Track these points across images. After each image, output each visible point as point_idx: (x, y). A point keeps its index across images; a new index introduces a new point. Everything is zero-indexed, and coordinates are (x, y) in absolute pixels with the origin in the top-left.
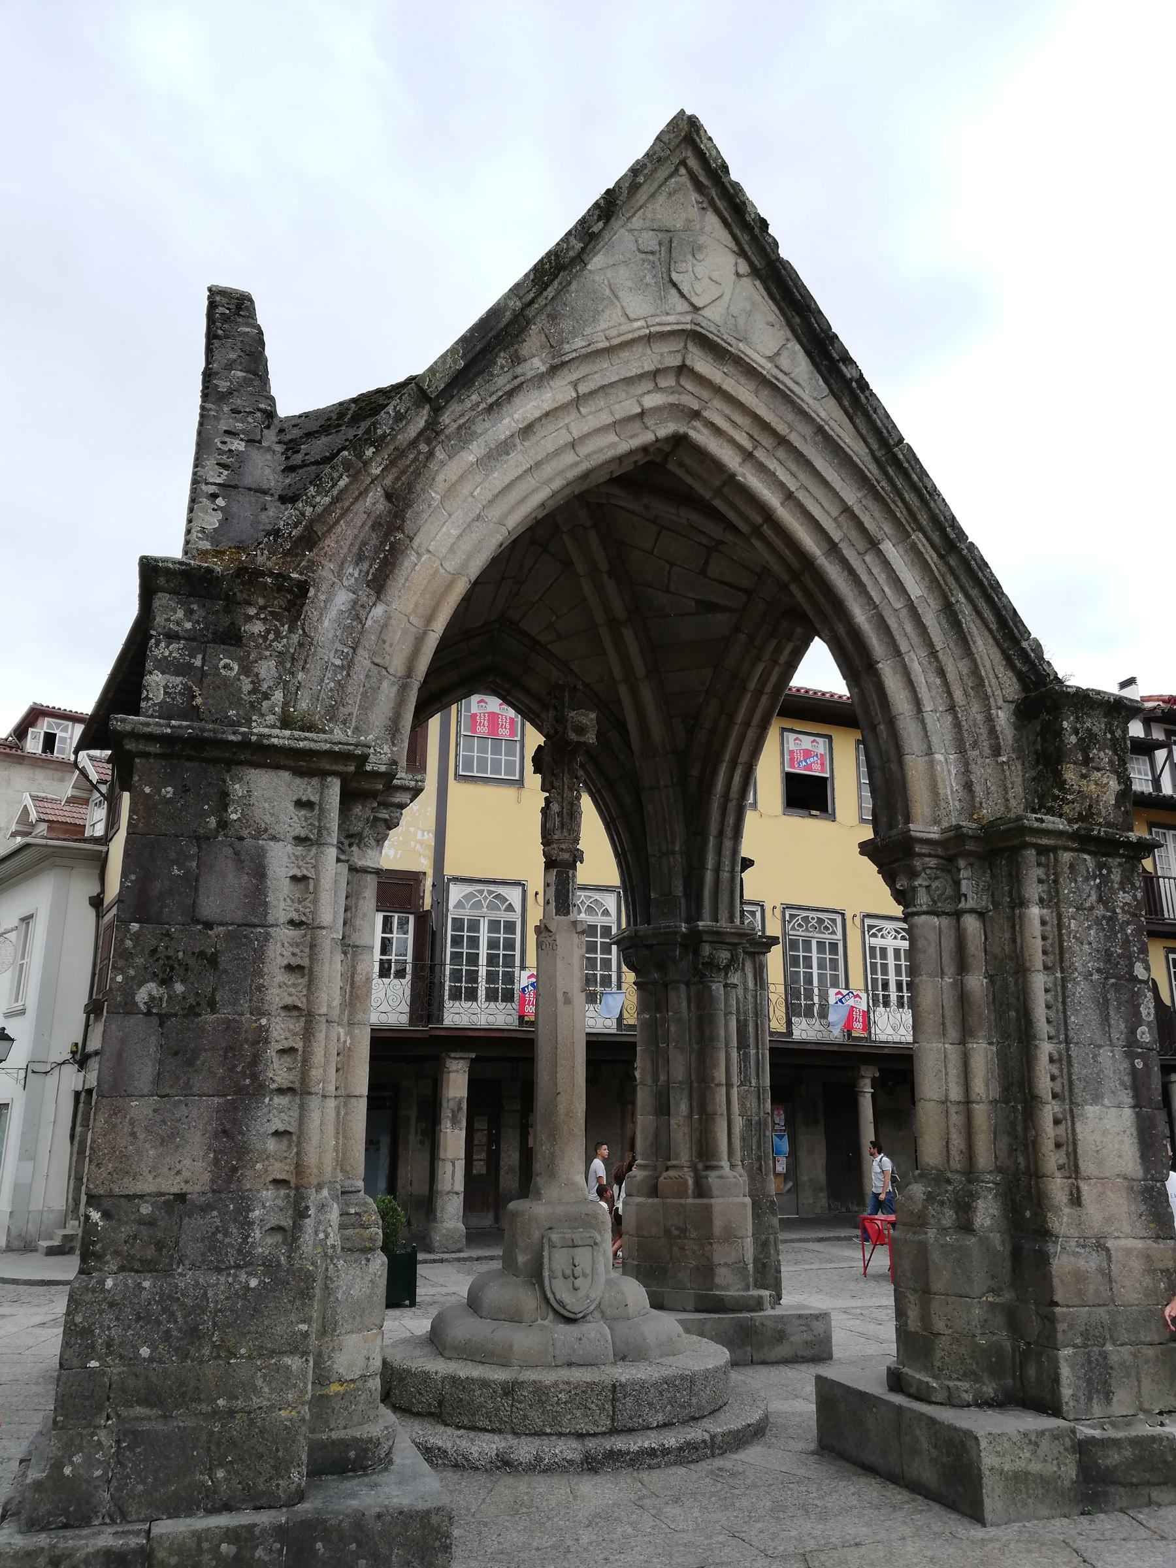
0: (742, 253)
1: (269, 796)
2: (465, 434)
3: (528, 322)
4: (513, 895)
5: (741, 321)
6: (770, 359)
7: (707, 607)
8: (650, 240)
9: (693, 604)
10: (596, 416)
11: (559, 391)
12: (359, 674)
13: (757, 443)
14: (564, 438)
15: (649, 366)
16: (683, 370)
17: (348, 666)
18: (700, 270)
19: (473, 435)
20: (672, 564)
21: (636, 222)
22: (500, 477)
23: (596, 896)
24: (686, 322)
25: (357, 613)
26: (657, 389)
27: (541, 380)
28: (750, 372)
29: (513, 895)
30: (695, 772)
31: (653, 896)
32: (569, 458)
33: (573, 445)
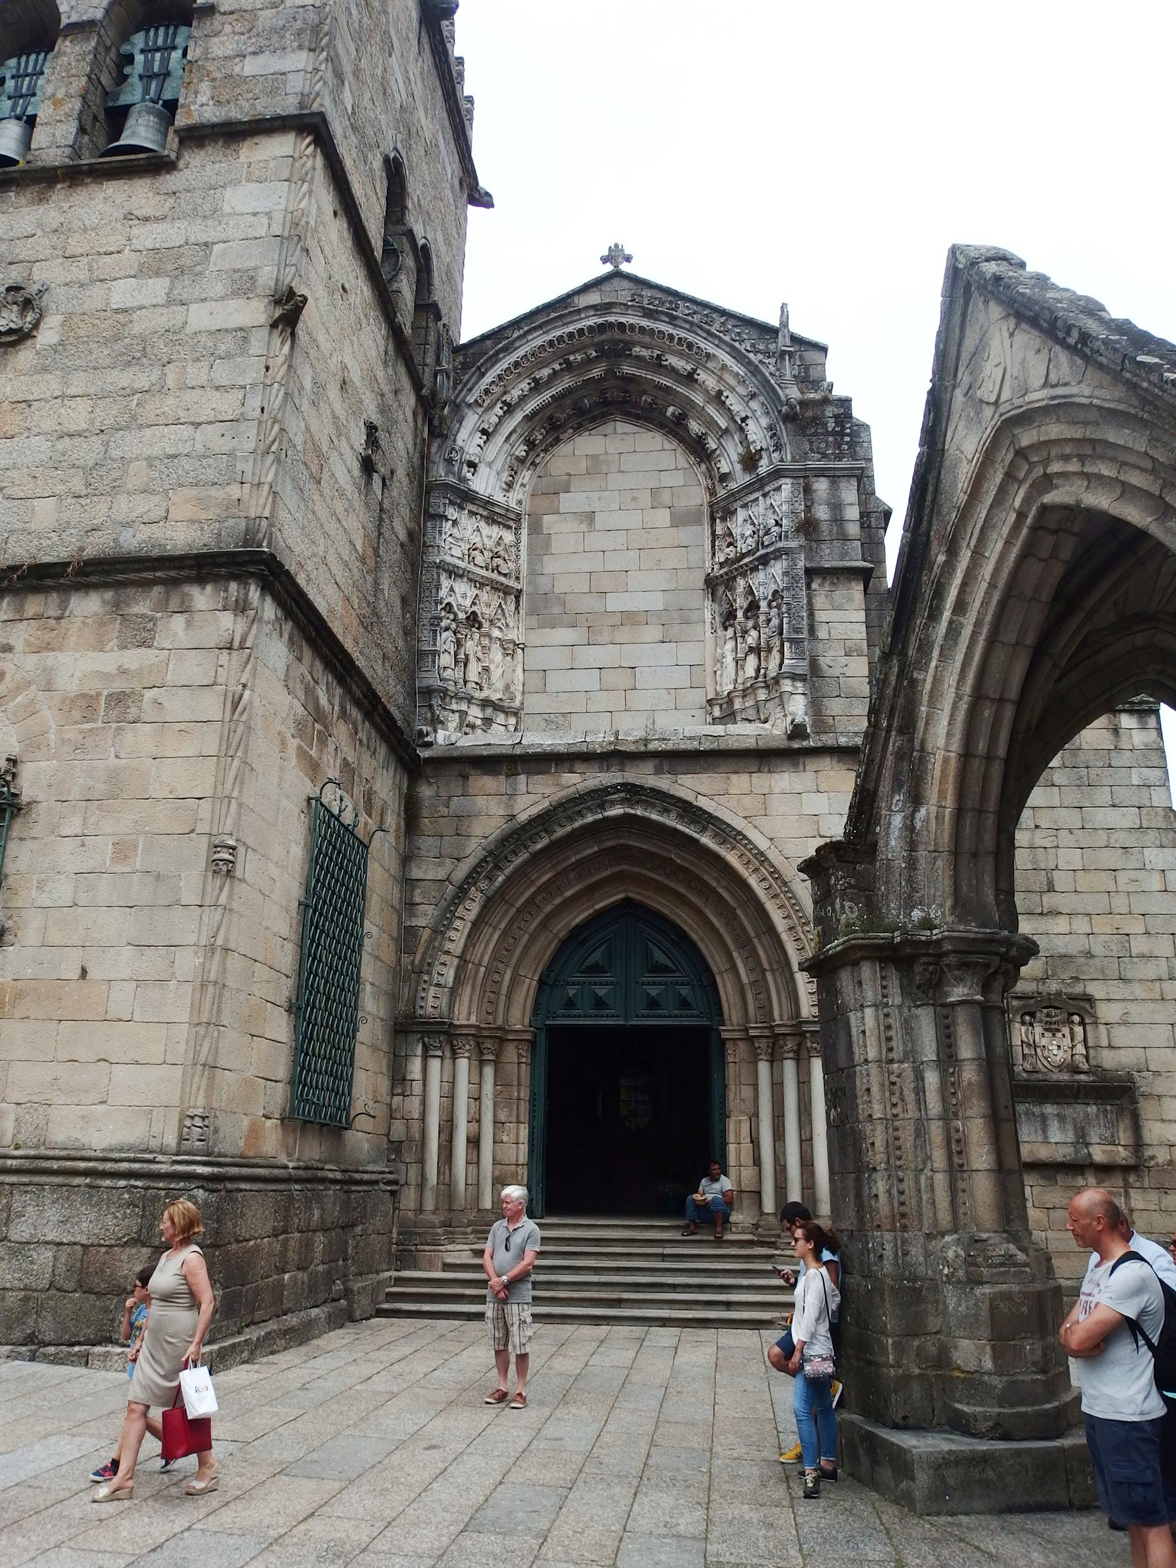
2: (925, 649)
3: (928, 535)
5: (1021, 377)
6: (1046, 384)
10: (995, 548)
12: (922, 865)
13: (1082, 459)
14: (984, 586)
15: (998, 477)
16: (1021, 453)
17: (912, 863)
24: (997, 421)
25: (909, 826)
26: (1021, 482)
27: (950, 565)
33: (992, 585)
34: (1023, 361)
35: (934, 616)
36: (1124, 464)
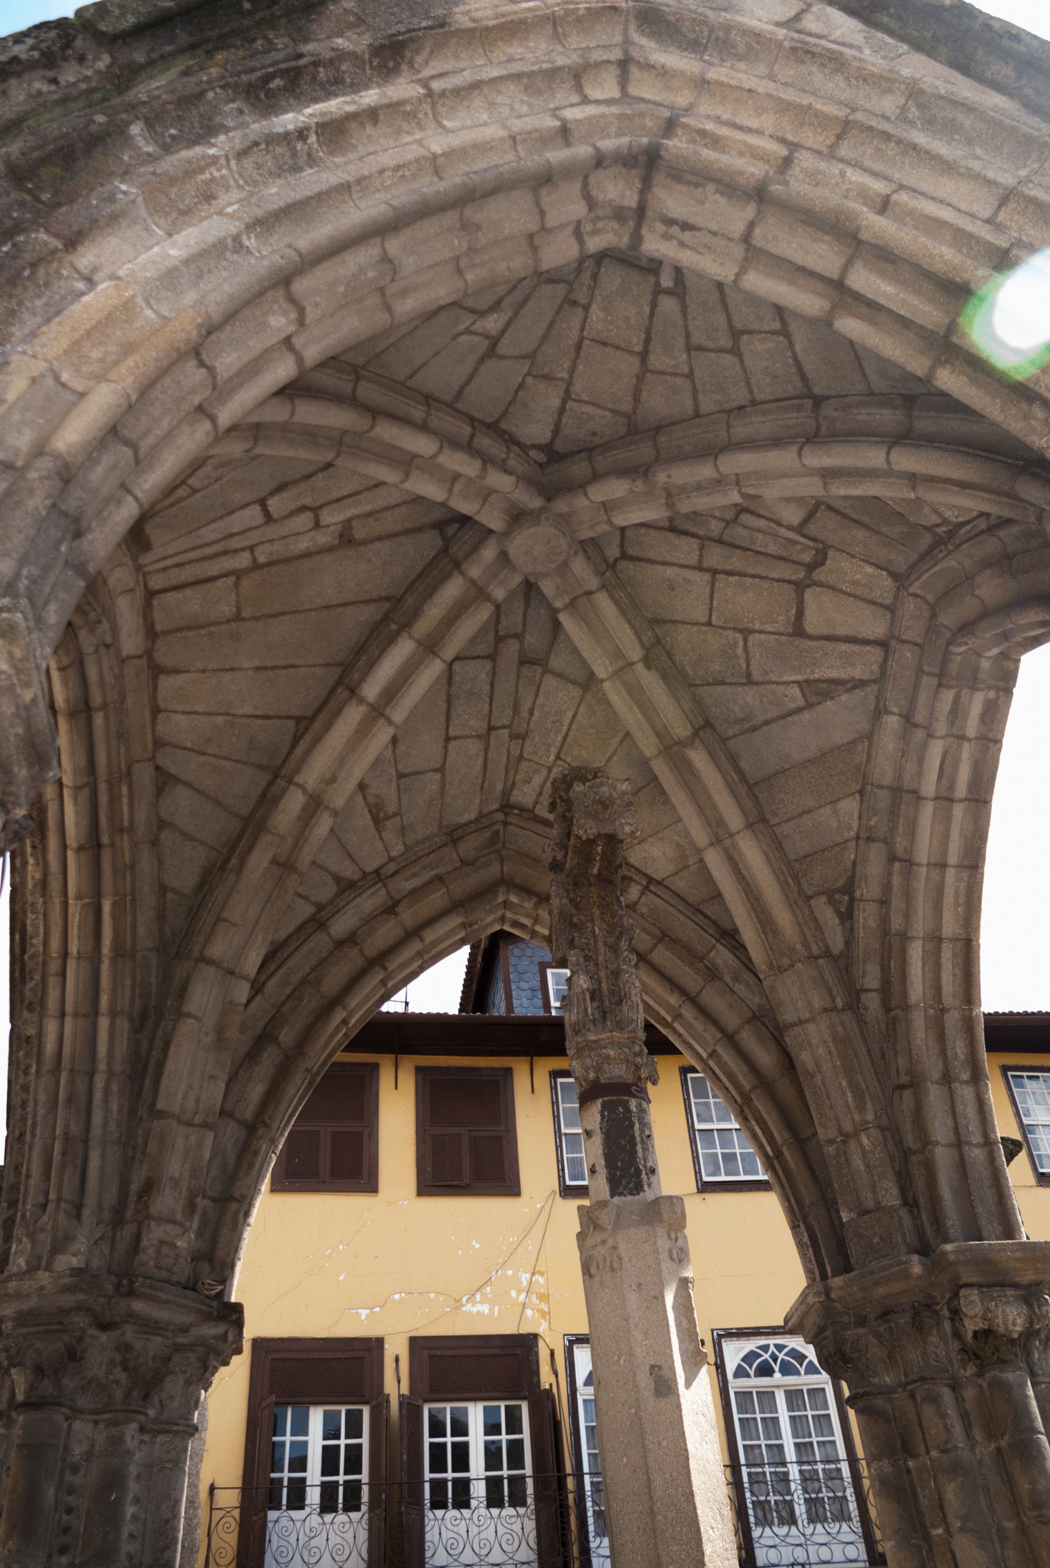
7: (819, 692)
9: (796, 691)
20: (746, 633)
30: (872, 979)
31: (845, 1216)
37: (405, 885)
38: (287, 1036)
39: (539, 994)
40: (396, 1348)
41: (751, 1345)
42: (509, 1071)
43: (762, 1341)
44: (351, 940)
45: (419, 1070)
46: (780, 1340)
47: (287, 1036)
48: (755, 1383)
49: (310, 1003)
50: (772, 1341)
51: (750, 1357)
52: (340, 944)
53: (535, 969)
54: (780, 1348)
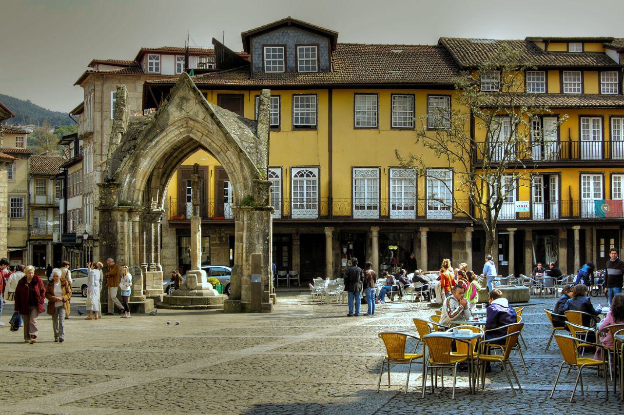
0: (196, 99)
1: (117, 215)
2: (146, 146)
4: (278, 172)
8: (178, 100)
11: (164, 134)
13: (203, 135)
18: (188, 105)
19: (147, 146)
21: (176, 97)
22: (153, 152)
23: (309, 169)
25: (130, 182)
26: (183, 127)
28: (198, 122)
29: (278, 172)
32: (167, 144)
34: (198, 111)
35: (151, 141)
36: (213, 141)
37: (184, 147)
38: (168, 172)
39: (261, 56)
40: (211, 168)
41: (300, 170)
42: (243, 96)
43: (303, 169)
44: (176, 157)
45: (218, 95)
46: (307, 169)
47: (168, 172)
48: (298, 179)
49: (171, 167)
50: (305, 169)
51: (299, 173)
52: (175, 158)
53: (260, 47)
54: (307, 171)
